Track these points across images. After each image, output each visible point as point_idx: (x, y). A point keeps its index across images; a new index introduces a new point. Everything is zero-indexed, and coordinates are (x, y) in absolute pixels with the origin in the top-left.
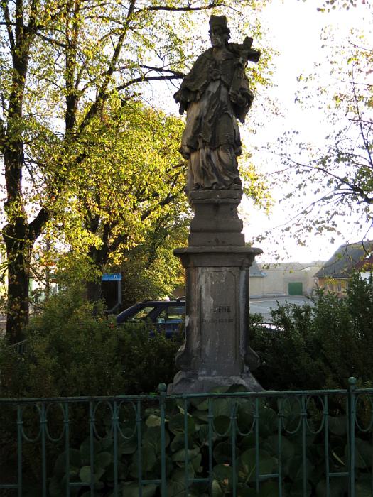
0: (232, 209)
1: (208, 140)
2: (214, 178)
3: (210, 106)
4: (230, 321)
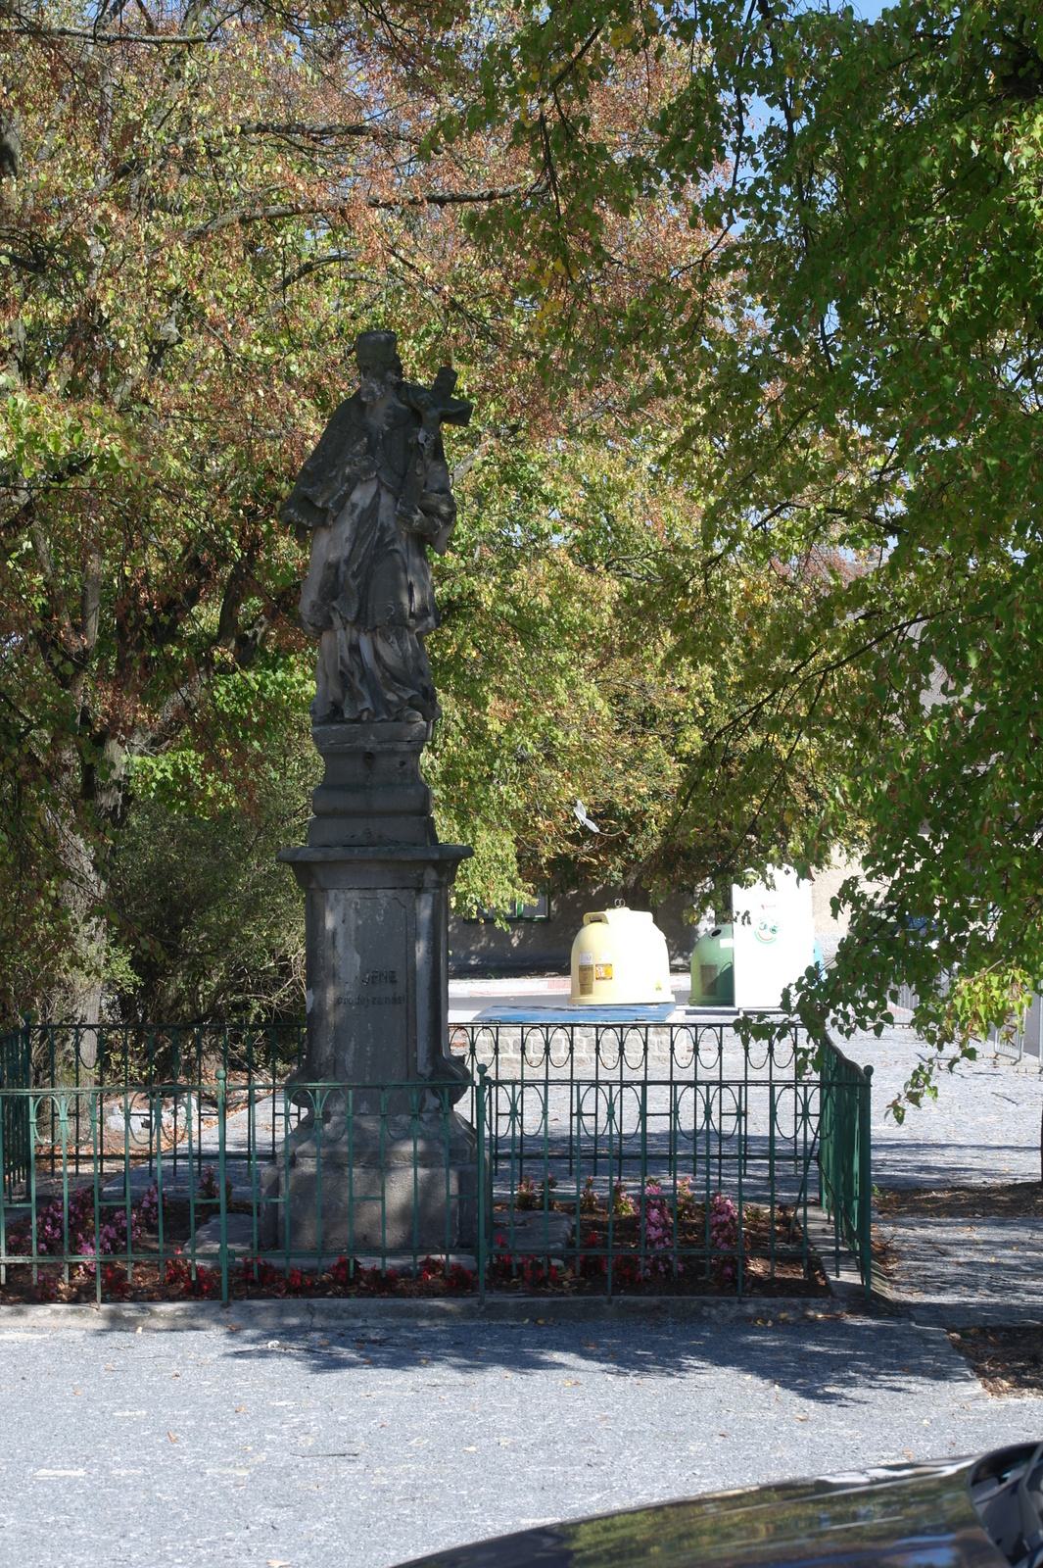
0: (403, 764)
1: (351, 618)
2: (363, 699)
3: (357, 539)
4: (395, 1001)
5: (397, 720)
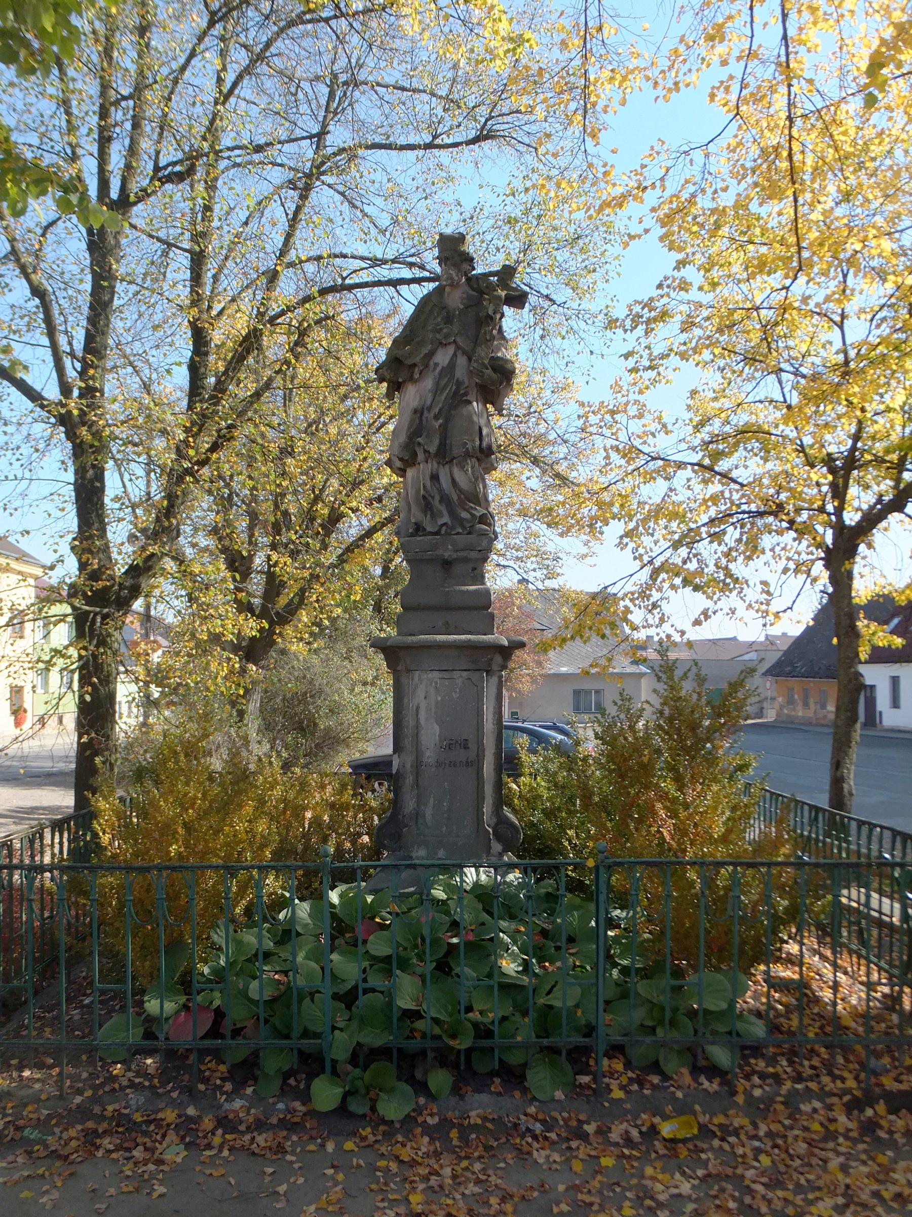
0: (474, 569)
1: (433, 449)
3: (437, 390)
4: (468, 764)
5: (469, 533)
